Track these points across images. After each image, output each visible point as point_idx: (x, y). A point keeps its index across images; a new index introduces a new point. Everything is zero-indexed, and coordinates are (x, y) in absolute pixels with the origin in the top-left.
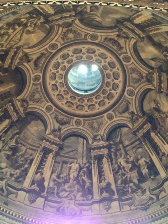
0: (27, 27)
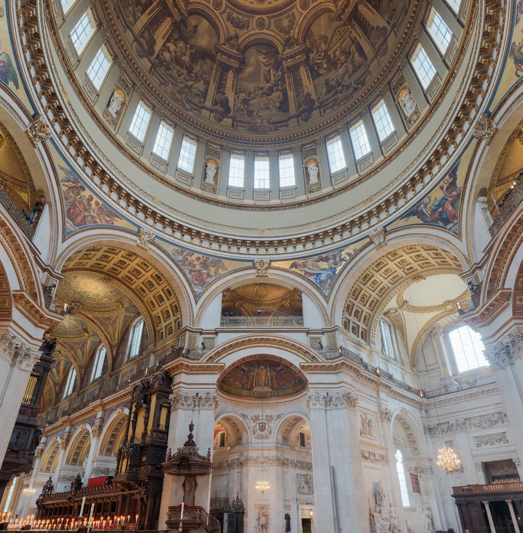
0: (326, 51)
